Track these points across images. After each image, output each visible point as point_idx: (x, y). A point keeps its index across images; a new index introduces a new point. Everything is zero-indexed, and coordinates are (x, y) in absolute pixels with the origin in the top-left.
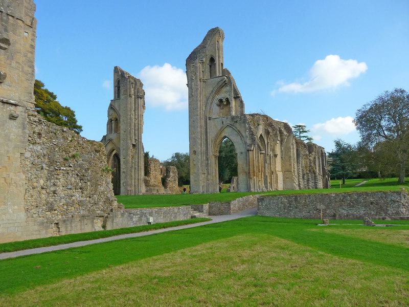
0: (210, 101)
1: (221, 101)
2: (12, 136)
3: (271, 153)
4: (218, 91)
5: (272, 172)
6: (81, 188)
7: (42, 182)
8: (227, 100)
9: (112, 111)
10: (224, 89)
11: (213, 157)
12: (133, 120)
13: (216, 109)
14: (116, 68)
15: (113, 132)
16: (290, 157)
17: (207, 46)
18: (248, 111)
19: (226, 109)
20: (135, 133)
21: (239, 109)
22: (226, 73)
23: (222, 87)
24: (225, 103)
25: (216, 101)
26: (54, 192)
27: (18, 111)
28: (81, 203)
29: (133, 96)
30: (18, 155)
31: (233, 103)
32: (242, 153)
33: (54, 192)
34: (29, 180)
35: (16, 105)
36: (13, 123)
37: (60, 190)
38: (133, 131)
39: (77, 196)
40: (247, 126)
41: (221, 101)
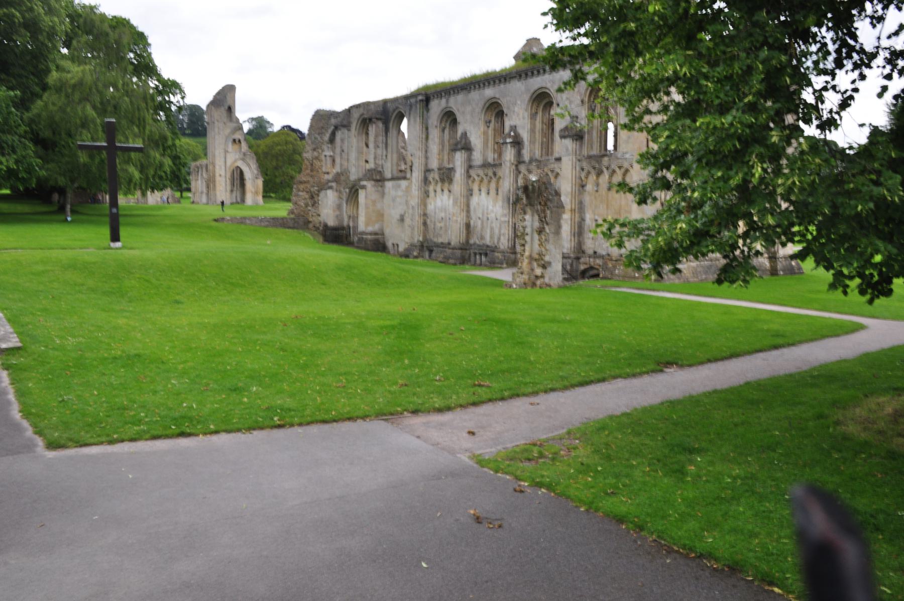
1: (234, 141)
8: (239, 141)
19: (236, 147)
22: (237, 120)
41: (234, 141)
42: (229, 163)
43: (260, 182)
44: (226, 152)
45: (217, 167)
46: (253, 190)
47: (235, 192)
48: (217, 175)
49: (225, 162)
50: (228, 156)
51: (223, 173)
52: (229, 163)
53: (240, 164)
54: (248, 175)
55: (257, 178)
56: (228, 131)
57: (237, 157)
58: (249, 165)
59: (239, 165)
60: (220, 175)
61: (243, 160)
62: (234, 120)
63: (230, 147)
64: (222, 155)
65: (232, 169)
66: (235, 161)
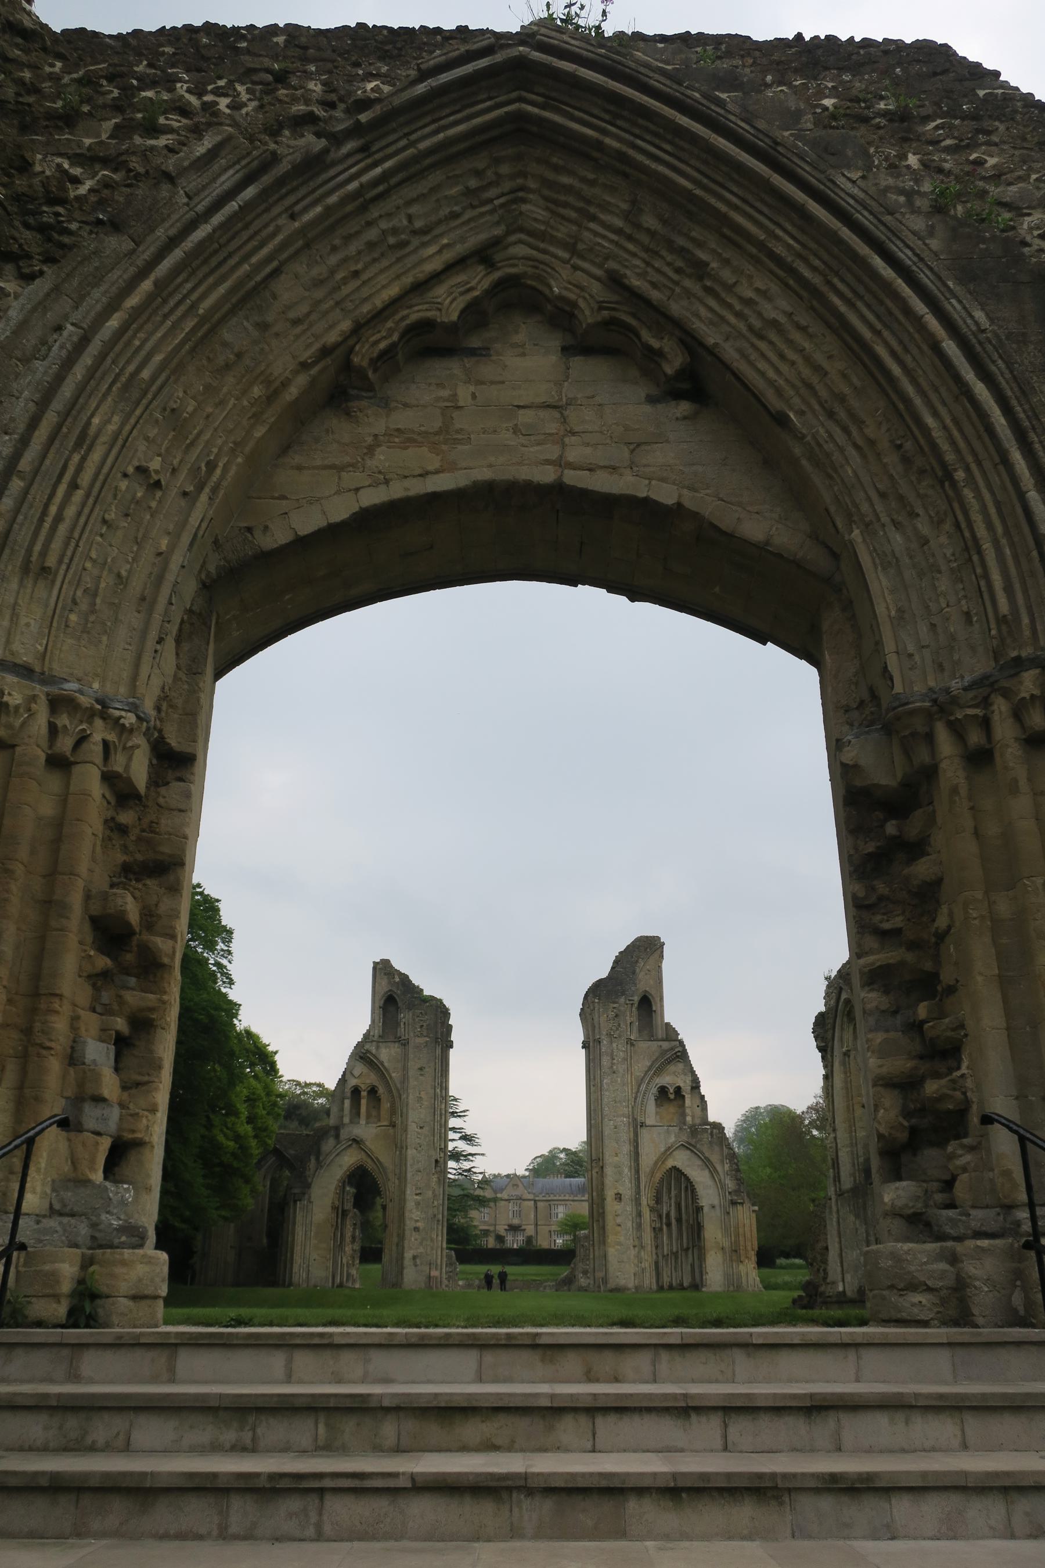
0: (643, 1087)
1: (663, 1091)
4: (659, 1071)
8: (678, 1089)
9: (360, 1068)
10: (672, 1068)
13: (651, 1106)
15: (363, 1121)
17: (638, 970)
19: (671, 1109)
21: (698, 1111)
22: (671, 1033)
23: (669, 1061)
24: (672, 1097)
32: (713, 1207)
40: (726, 1151)
41: (663, 1091)
42: (647, 1160)
43: (746, 1216)
44: (637, 1126)
45: (609, 1171)
46: (727, 1244)
47: (690, 1252)
48: (610, 1194)
49: (636, 1155)
50: (645, 1135)
51: (626, 1189)
52: (647, 1160)
53: (681, 1160)
54: (708, 1194)
55: (734, 1203)
56: (641, 1065)
57: (672, 1139)
58: (707, 1163)
59: (679, 1165)
60: (619, 1197)
61: (687, 1147)
62: (660, 1033)
63: (651, 1112)
64: (625, 1135)
65: (658, 1175)
66: (668, 1152)
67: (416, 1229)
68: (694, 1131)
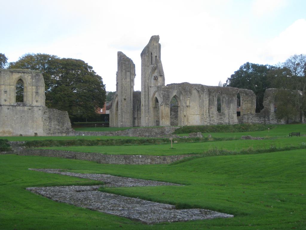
2: (40, 114)
3: (184, 105)
5: (185, 116)
6: (59, 125)
7: (47, 124)
11: (152, 107)
12: (124, 85)
13: (153, 81)
14: (118, 52)
16: (204, 106)
18: (168, 81)
20: (125, 92)
24: (157, 79)
25: (153, 78)
26: (51, 126)
27: (41, 108)
28: (58, 129)
29: (124, 71)
30: (41, 118)
31: (160, 79)
33: (51, 126)
34: (44, 123)
35: (40, 107)
36: (40, 111)
37: (52, 125)
38: (124, 91)
39: (57, 127)
67: (119, 114)
68: (158, 87)
